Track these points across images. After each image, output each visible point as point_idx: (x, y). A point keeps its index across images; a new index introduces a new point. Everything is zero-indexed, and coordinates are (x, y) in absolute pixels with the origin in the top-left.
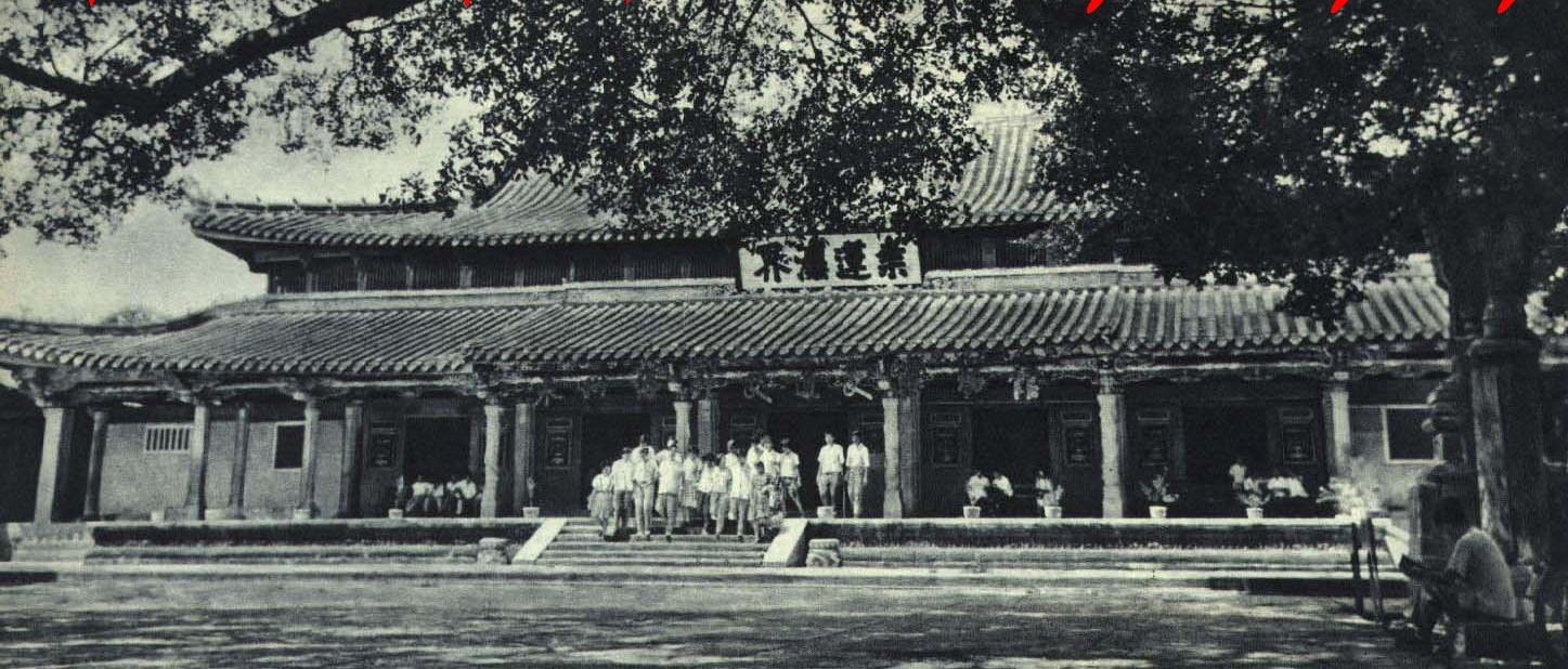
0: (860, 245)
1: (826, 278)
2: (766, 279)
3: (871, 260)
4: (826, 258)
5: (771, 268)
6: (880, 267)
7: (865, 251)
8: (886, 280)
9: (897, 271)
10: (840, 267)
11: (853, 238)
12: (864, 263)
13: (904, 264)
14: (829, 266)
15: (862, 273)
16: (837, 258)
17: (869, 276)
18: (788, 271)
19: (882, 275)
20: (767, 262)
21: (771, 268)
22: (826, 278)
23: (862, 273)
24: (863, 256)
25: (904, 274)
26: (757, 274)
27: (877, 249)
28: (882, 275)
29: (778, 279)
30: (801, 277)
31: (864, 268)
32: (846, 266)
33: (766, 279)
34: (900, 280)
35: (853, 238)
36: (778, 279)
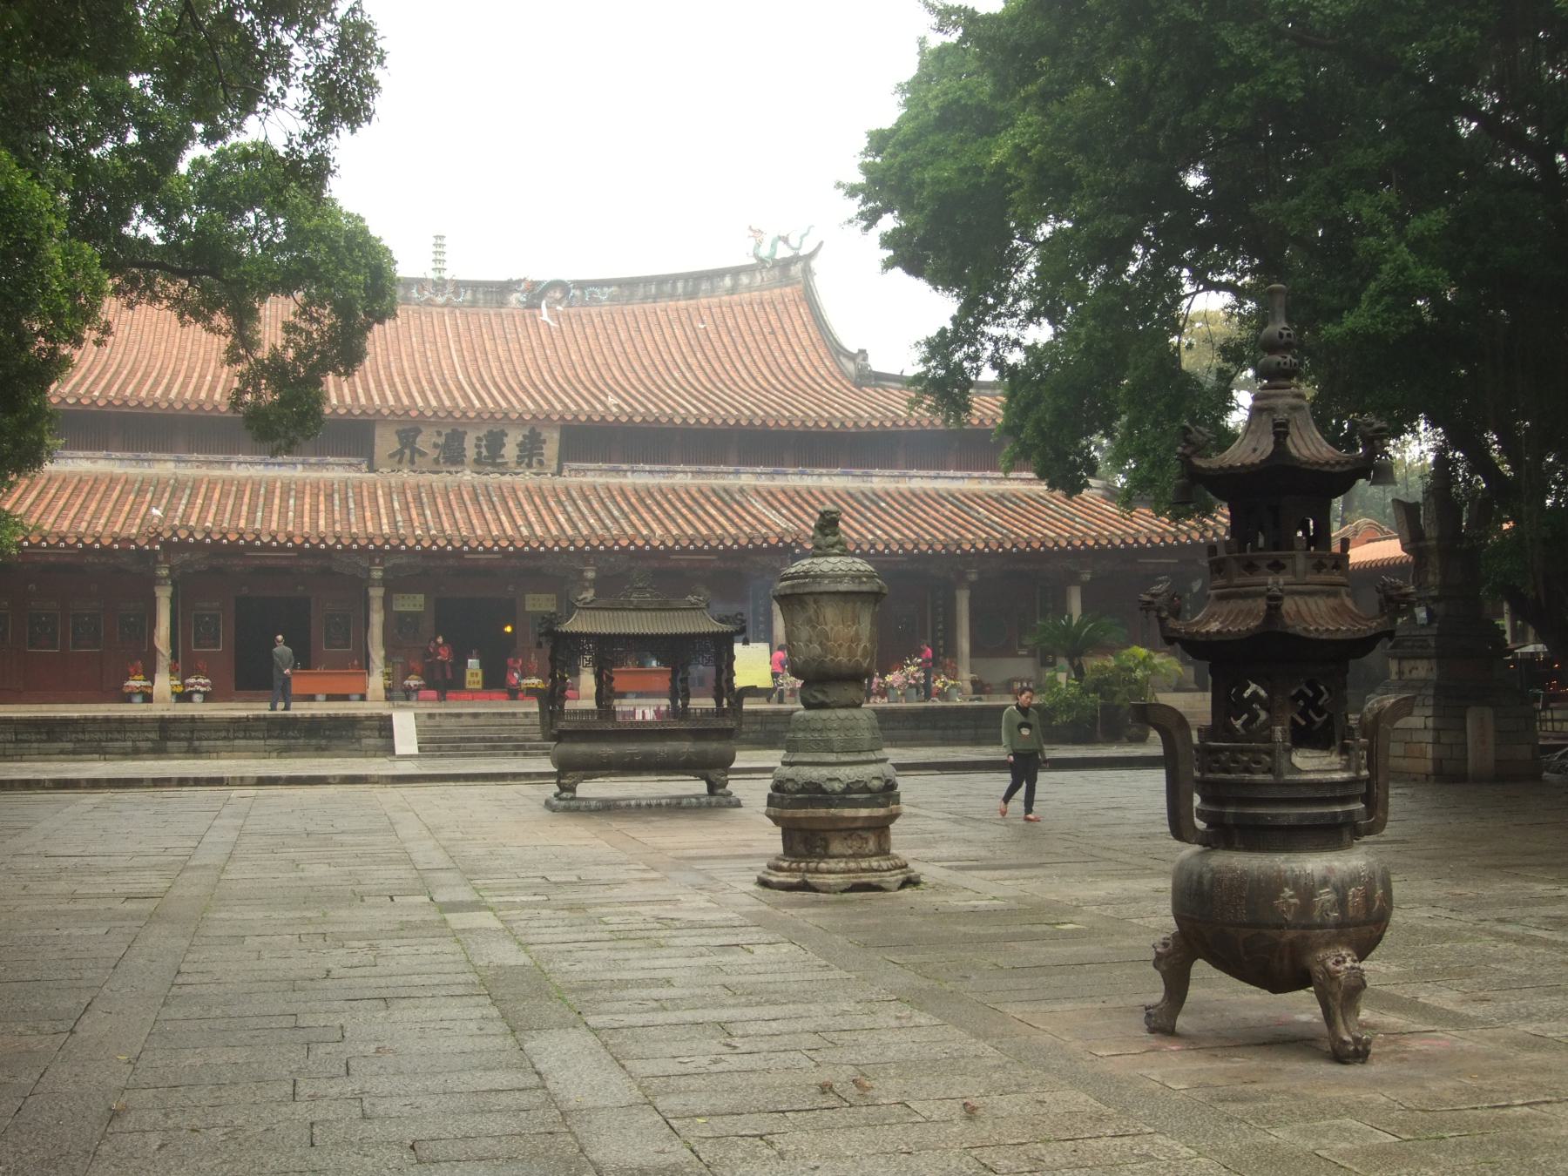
2: (400, 462)
3: (510, 451)
5: (407, 452)
7: (506, 440)
9: (535, 460)
10: (479, 453)
12: (503, 451)
13: (542, 455)
14: (467, 453)
15: (499, 461)
16: (478, 446)
17: (506, 463)
19: (519, 464)
20: (404, 446)
21: (407, 452)
23: (499, 461)
24: (504, 445)
25: (541, 463)
26: (392, 456)
27: (520, 438)
28: (519, 464)
29: (412, 462)
31: (503, 456)
32: (484, 452)
33: (400, 462)
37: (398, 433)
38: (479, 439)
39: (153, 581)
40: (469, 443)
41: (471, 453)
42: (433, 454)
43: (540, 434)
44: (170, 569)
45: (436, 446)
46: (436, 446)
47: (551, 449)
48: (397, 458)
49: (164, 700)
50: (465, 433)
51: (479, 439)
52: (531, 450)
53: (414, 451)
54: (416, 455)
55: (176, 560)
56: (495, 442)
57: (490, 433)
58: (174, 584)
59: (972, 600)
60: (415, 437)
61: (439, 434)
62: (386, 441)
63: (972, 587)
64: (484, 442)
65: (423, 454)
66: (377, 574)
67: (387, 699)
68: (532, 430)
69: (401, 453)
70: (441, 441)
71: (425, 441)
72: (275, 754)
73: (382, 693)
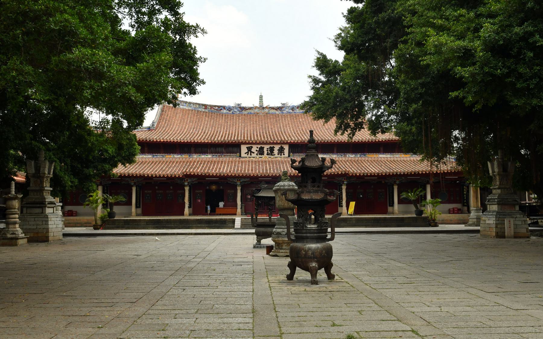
0: (274, 147)
1: (264, 155)
2: (248, 155)
3: (276, 152)
4: (264, 150)
5: (249, 152)
6: (278, 153)
7: (274, 149)
8: (279, 156)
9: (282, 154)
10: (268, 152)
11: (272, 146)
13: (284, 152)
15: (273, 154)
16: (267, 151)
17: (275, 155)
18: (254, 153)
20: (248, 151)
21: (249, 152)
22: (264, 155)
23: (273, 154)
25: (284, 154)
26: (245, 153)
28: (278, 155)
29: (251, 155)
30: (257, 154)
32: (269, 152)
33: (248, 155)
34: (283, 156)
35: (272, 146)
36: (251, 155)
37: (247, 147)
38: (267, 149)
39: (184, 186)
40: (265, 150)
41: (266, 152)
42: (256, 152)
43: (283, 147)
44: (188, 183)
45: (257, 151)
46: (257, 151)
47: (286, 151)
48: (247, 154)
49: (187, 215)
50: (264, 147)
51: (267, 149)
52: (281, 151)
53: (251, 152)
54: (252, 153)
55: (189, 180)
56: (272, 150)
57: (270, 147)
58: (190, 186)
59: (398, 188)
60: (251, 149)
61: (257, 148)
62: (244, 149)
63: (398, 185)
64: (269, 150)
65: (254, 153)
66: (238, 183)
67: (242, 215)
68: (281, 146)
69: (248, 153)
70: (258, 149)
71: (255, 149)
72: (207, 228)
73: (240, 213)
